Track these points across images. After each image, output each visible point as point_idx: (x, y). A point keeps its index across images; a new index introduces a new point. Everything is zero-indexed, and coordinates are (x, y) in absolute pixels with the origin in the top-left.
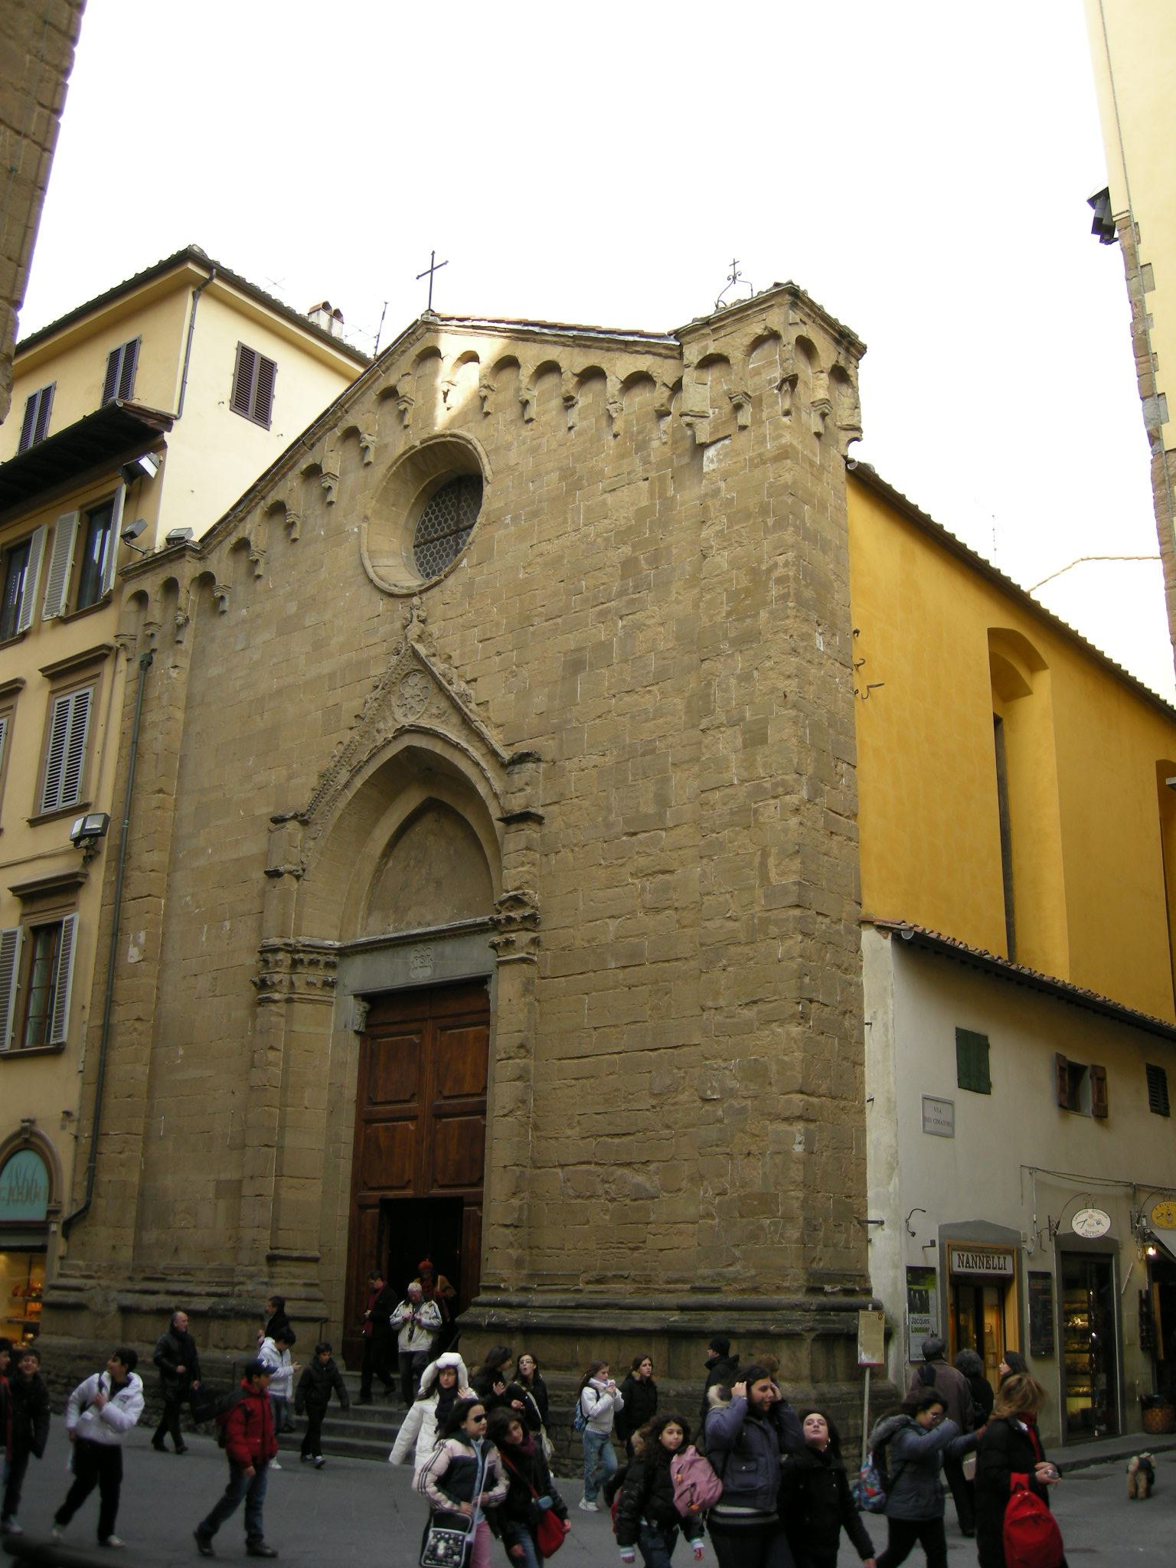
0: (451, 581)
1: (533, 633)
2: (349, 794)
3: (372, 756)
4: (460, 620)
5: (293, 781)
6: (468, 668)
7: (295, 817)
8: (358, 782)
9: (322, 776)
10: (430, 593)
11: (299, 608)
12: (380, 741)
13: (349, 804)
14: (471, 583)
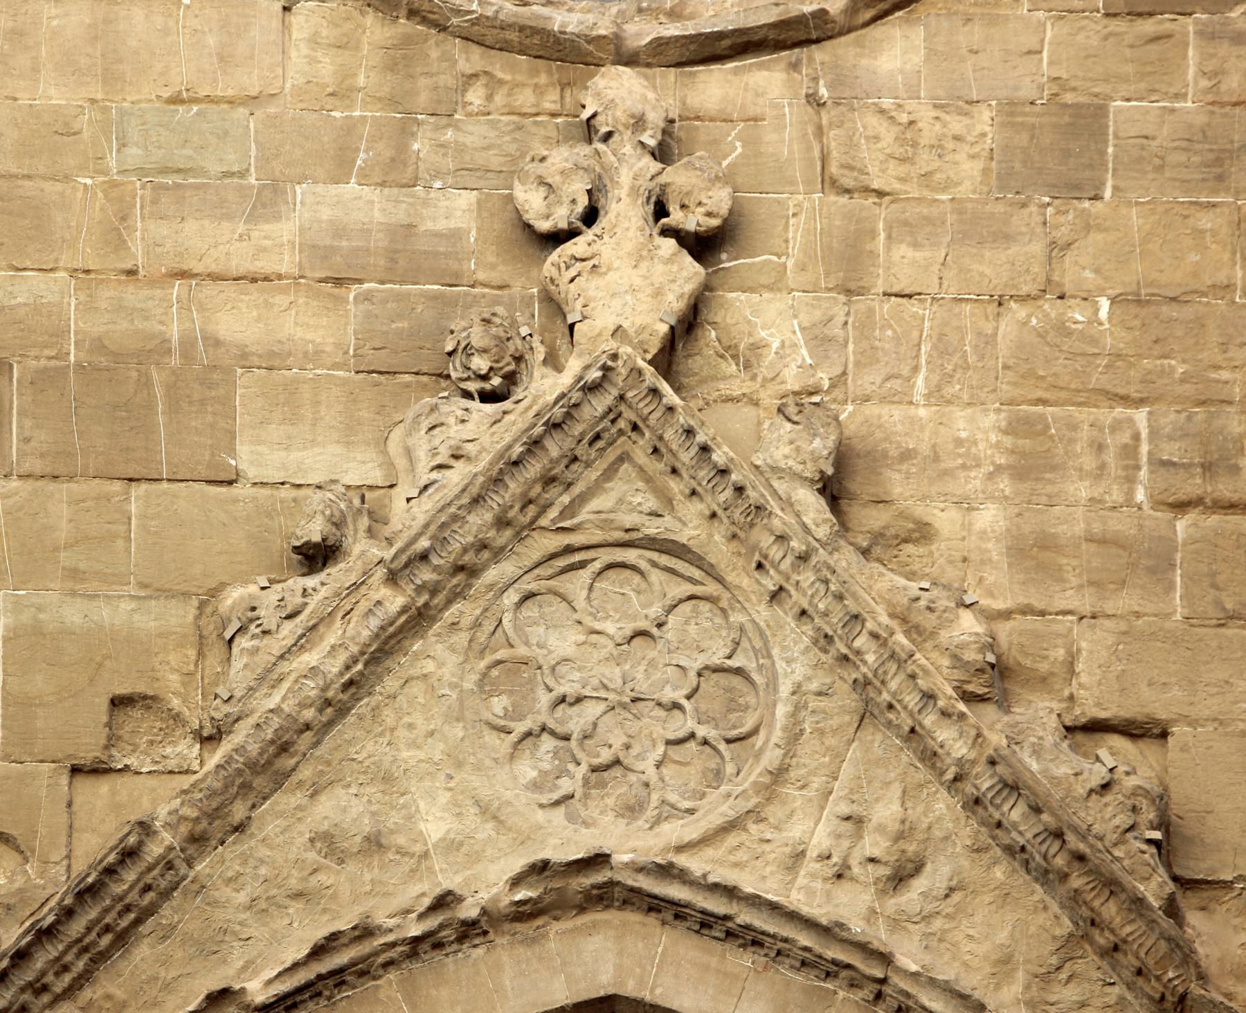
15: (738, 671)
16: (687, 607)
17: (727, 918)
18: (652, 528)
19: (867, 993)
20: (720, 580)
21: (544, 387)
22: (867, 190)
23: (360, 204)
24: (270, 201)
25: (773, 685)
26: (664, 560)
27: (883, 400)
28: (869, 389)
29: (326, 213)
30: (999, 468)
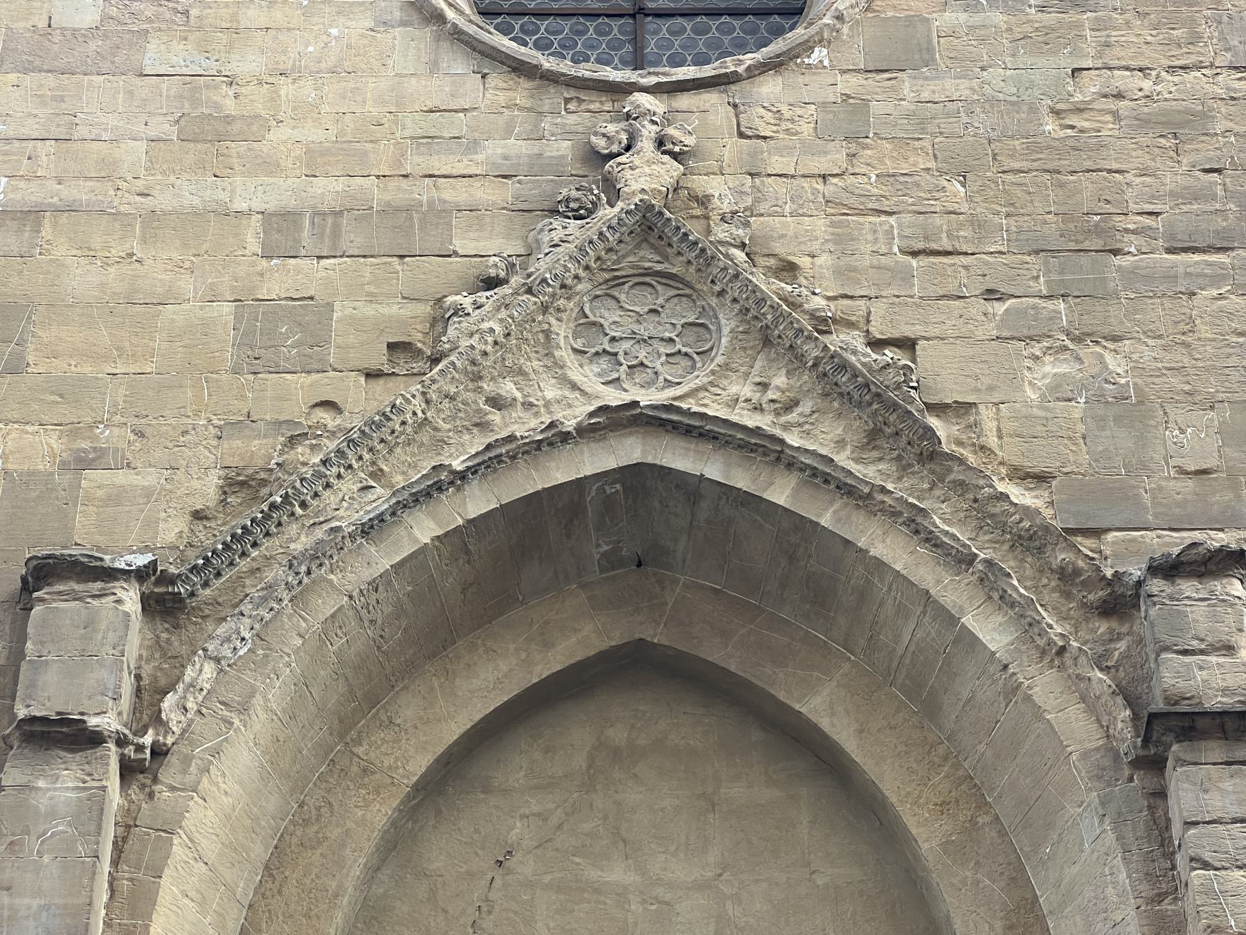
0: (769, 87)
1: (1130, 275)
2: (382, 558)
3: (489, 463)
4: (820, 187)
5: (92, 478)
6: (878, 309)
7: (141, 575)
8: (423, 529)
9: (240, 484)
10: (684, 101)
11: (106, 18)
12: (525, 426)
13: (374, 585)
14: (855, 106)
15: (702, 325)
16: (675, 300)
17: (701, 427)
18: (659, 267)
19: (773, 457)
20: (692, 288)
21: (607, 213)
22: (758, 137)
23: (519, 148)
24: (474, 146)
25: (719, 330)
26: (664, 281)
27: (769, 215)
28: (762, 211)
29: (499, 151)
30: (827, 241)
